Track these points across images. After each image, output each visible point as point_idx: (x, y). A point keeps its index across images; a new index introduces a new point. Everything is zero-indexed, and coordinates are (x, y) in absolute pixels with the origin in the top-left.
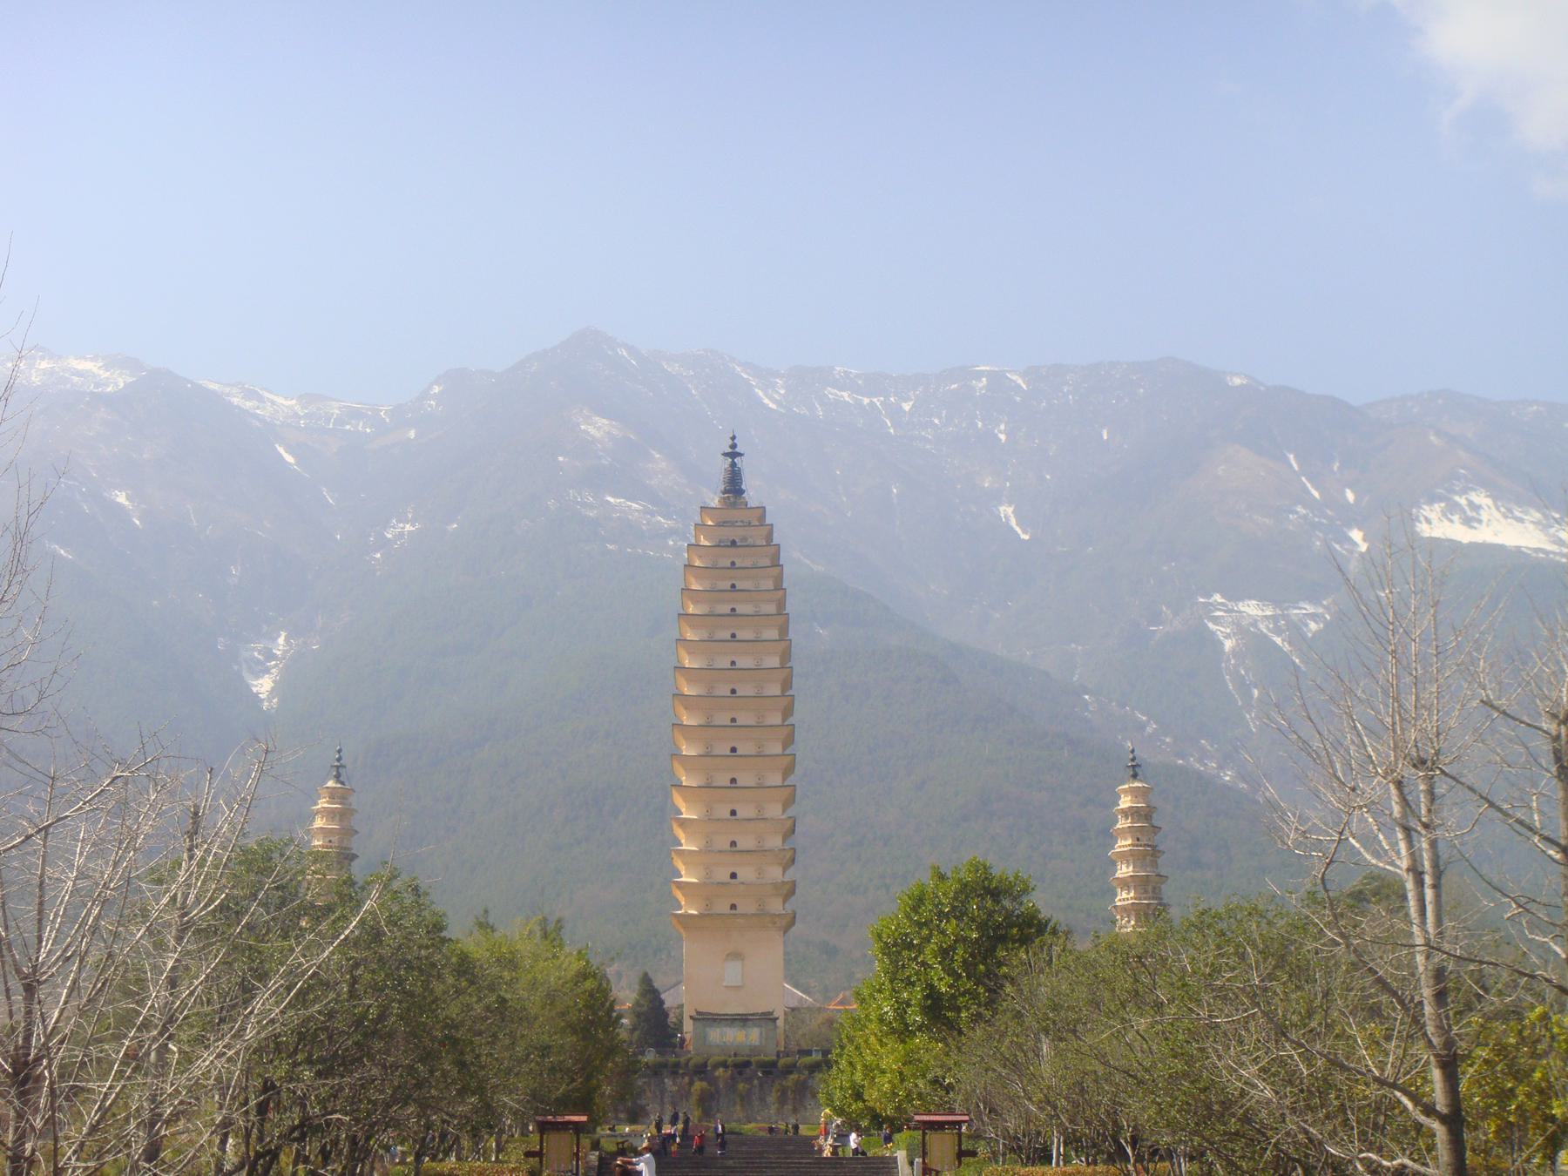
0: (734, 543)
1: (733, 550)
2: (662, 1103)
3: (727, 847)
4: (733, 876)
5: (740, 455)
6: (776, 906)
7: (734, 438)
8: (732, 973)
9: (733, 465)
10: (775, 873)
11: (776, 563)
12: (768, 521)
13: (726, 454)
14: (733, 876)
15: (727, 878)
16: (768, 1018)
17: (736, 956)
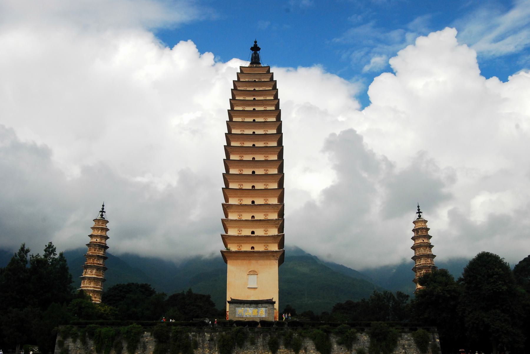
0: (255, 81)
1: (255, 84)
2: (203, 348)
3: (250, 218)
4: (253, 233)
5: (259, 49)
6: (274, 248)
7: (256, 42)
8: (252, 281)
9: (255, 53)
10: (274, 232)
11: (275, 88)
12: (271, 72)
13: (252, 49)
14: (253, 233)
15: (250, 234)
16: (271, 302)
17: (254, 273)
